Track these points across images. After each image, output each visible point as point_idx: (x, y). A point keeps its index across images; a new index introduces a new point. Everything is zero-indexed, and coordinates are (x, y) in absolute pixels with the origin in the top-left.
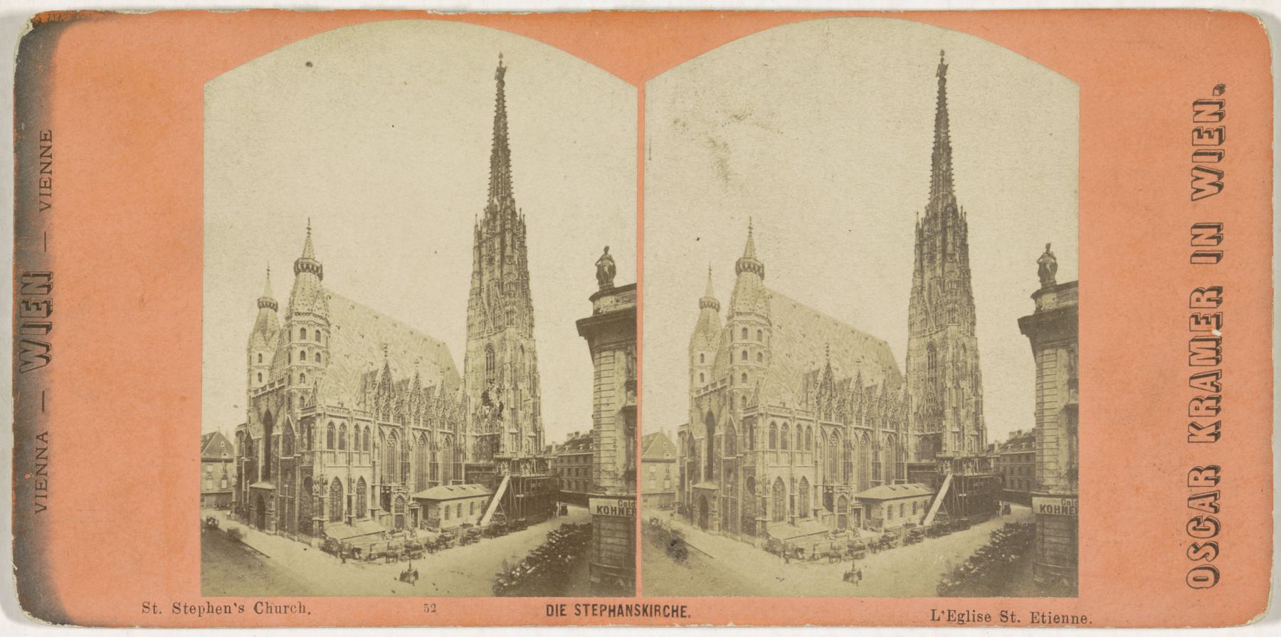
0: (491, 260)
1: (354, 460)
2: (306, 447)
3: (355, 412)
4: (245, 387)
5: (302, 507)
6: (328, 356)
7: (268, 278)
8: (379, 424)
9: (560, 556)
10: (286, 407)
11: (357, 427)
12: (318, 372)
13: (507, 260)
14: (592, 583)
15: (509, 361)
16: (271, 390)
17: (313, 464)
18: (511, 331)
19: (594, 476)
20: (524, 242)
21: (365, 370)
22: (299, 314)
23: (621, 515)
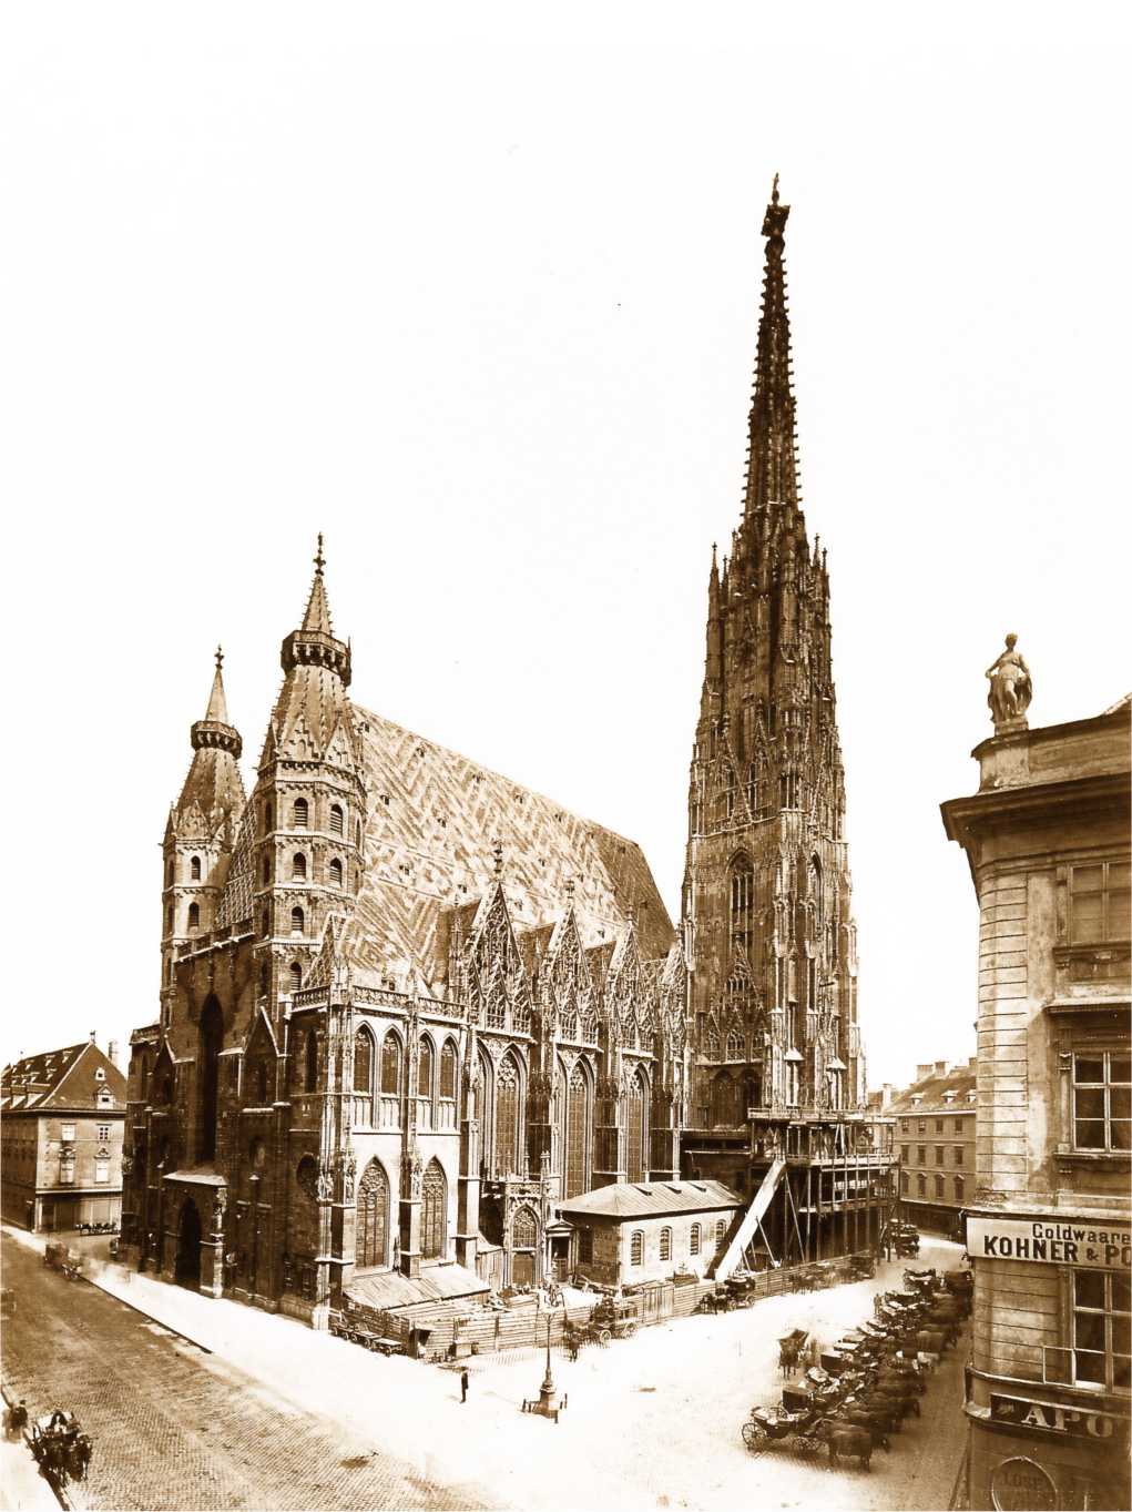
0: (746, 654)
2: (303, 1084)
3: (422, 1003)
6: (359, 868)
8: (478, 1033)
9: (900, 1354)
10: (257, 987)
11: (426, 1038)
13: (785, 656)
14: (975, 1421)
15: (785, 891)
16: (219, 945)
19: (978, 1169)
22: (292, 764)
23: (1040, 1259)
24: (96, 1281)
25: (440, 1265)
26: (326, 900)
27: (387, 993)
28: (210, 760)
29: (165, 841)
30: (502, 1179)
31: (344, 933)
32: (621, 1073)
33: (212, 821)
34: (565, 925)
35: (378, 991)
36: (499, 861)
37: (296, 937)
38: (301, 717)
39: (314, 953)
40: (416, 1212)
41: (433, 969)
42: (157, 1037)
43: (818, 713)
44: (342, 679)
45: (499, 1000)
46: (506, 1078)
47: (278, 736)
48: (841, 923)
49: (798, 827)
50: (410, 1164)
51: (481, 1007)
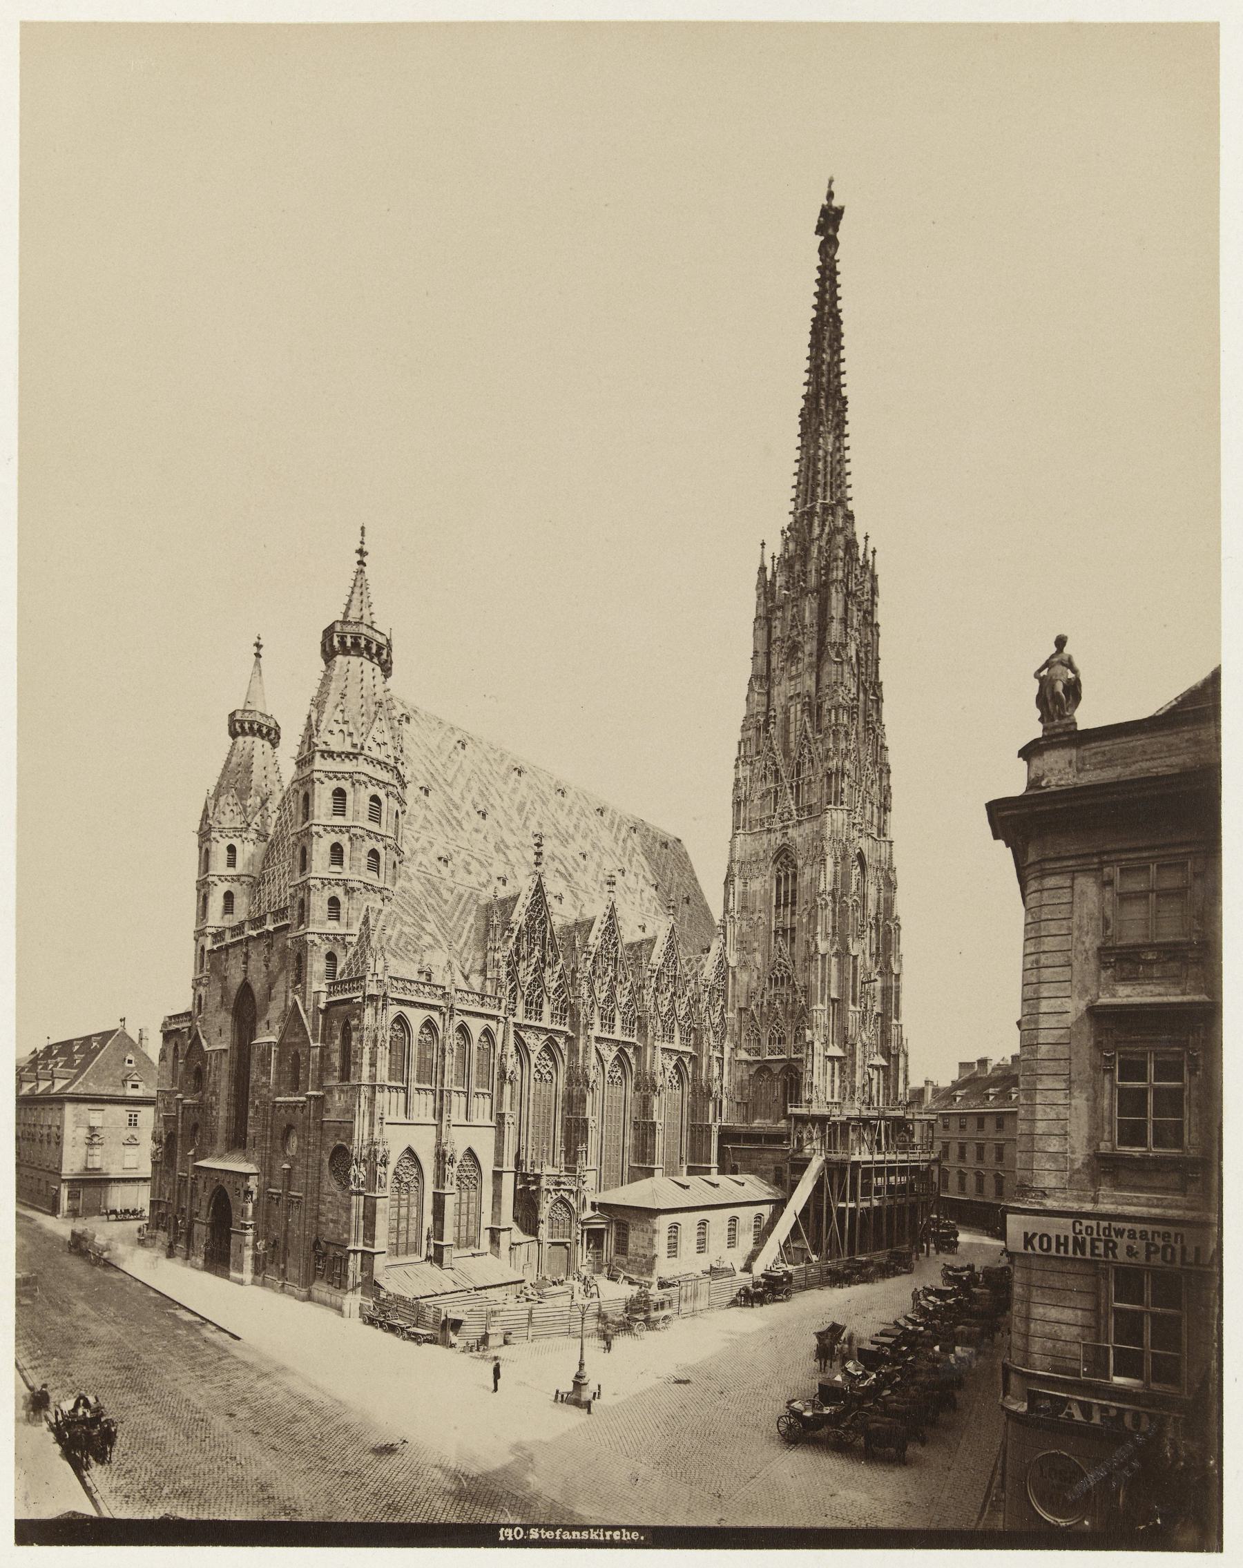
0: (794, 650)
1: (454, 1110)
2: (336, 1074)
4: (191, 925)
5: (323, 1219)
6: (397, 859)
7: (257, 664)
8: (515, 1025)
9: (937, 1348)
10: (292, 977)
11: (463, 1029)
12: (371, 895)
13: (833, 655)
14: (1012, 1415)
15: (829, 888)
16: (254, 933)
18: (836, 818)
19: (1018, 1166)
20: (871, 613)
21: (486, 896)
22: (331, 754)
23: (1079, 1255)
24: (124, 1267)
25: (473, 1255)
26: (363, 890)
27: (423, 984)
28: (247, 749)
29: (201, 829)
30: (537, 1171)
31: (380, 924)
32: (660, 1068)
33: (249, 810)
34: (605, 919)
35: (415, 982)
36: (539, 854)
37: (332, 927)
38: (341, 707)
39: (350, 943)
40: (450, 1202)
41: (471, 960)
42: (189, 1024)
43: (865, 712)
44: (382, 670)
45: (537, 993)
46: (544, 1071)
47: (317, 726)
48: (885, 920)
49: (843, 824)
50: (444, 1155)
51: (518, 999)
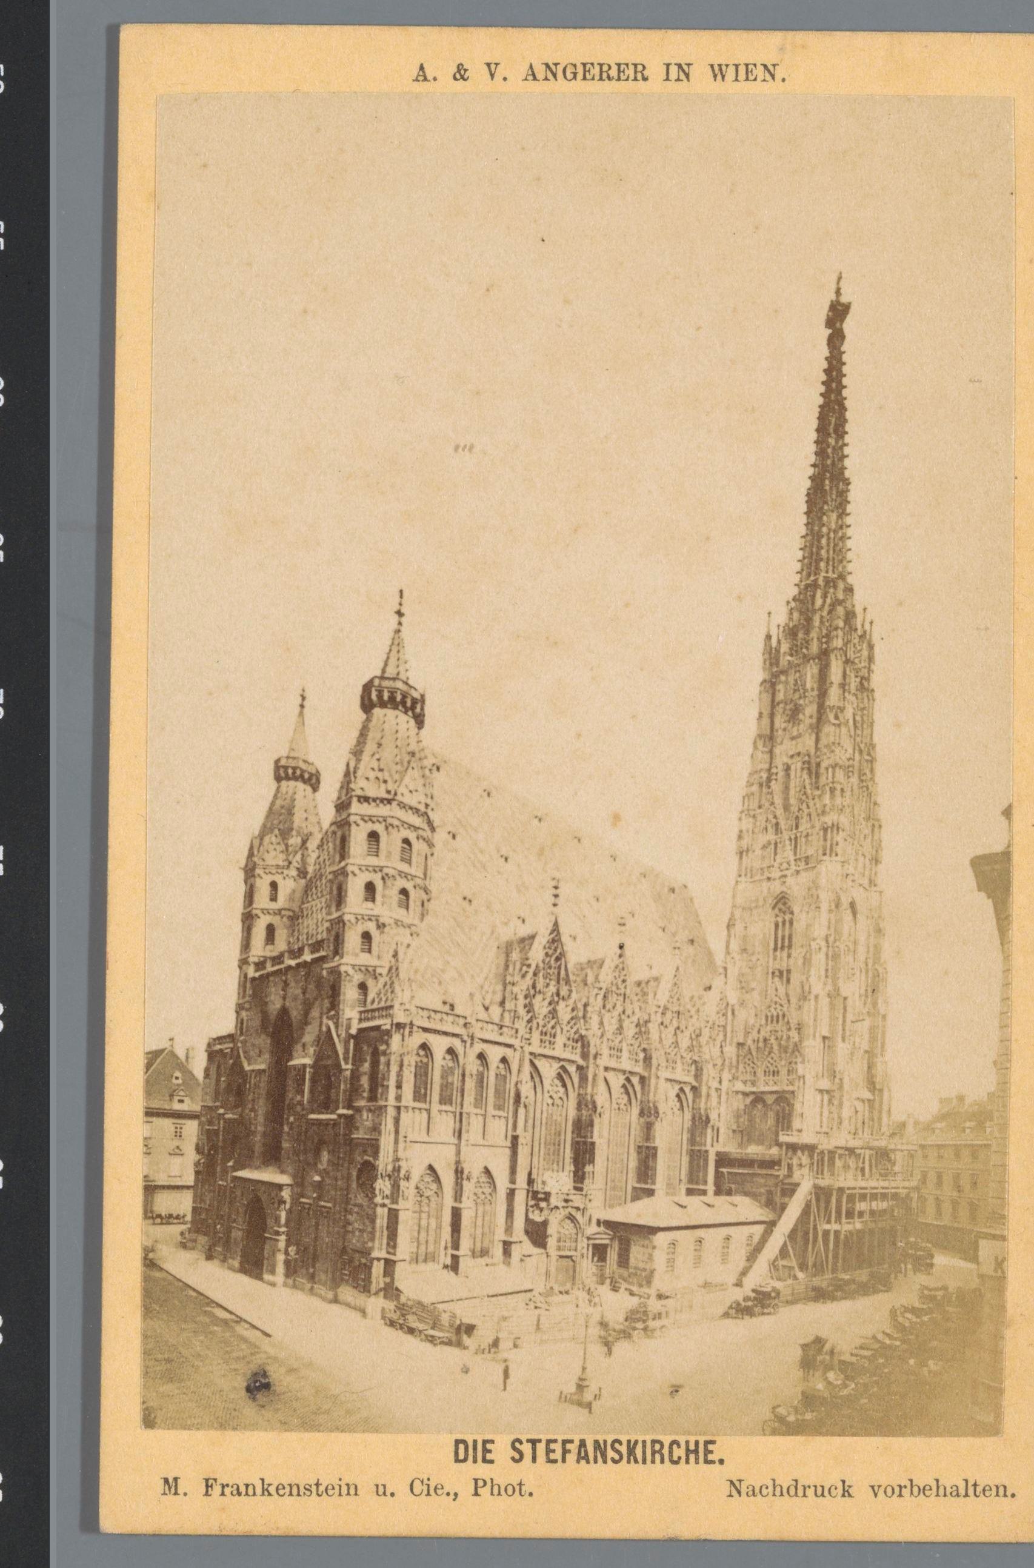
2: (365, 1095)
3: (480, 1024)
4: (235, 954)
6: (425, 897)
7: (301, 714)
8: (531, 1054)
10: (327, 1003)
11: (481, 1056)
12: (401, 930)
13: (831, 717)
16: (293, 963)
17: (380, 1133)
18: (829, 869)
20: (868, 679)
22: (366, 799)
24: (165, 1266)
26: (394, 926)
27: (447, 1014)
29: (246, 866)
33: (290, 849)
37: (364, 959)
38: (377, 756)
39: (380, 974)
42: (231, 1045)
43: (860, 770)
44: (416, 723)
46: (555, 1096)
47: (355, 772)
48: (874, 963)
50: (462, 1172)
51: (534, 1029)
